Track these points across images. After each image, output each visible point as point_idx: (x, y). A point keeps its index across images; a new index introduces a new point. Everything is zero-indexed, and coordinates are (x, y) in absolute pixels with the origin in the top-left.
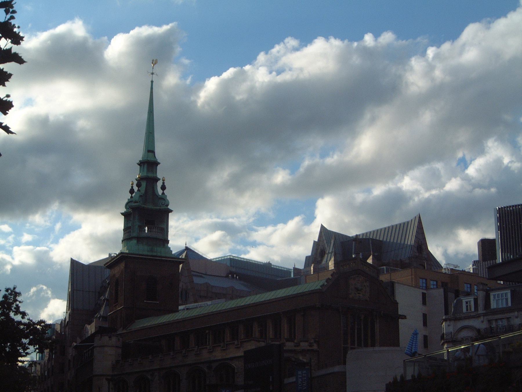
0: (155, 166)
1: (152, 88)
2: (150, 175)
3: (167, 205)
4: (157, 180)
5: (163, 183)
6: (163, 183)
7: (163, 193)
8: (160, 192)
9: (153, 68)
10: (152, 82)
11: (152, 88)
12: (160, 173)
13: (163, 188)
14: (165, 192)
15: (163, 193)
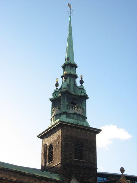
0: (75, 68)
1: (70, 21)
2: (72, 73)
3: (85, 93)
4: (76, 77)
5: (82, 79)
6: (82, 79)
7: (82, 86)
8: (79, 85)
9: (70, 9)
10: (70, 17)
11: (70, 21)
12: (78, 72)
13: (82, 82)
14: (83, 85)
15: (82, 86)
